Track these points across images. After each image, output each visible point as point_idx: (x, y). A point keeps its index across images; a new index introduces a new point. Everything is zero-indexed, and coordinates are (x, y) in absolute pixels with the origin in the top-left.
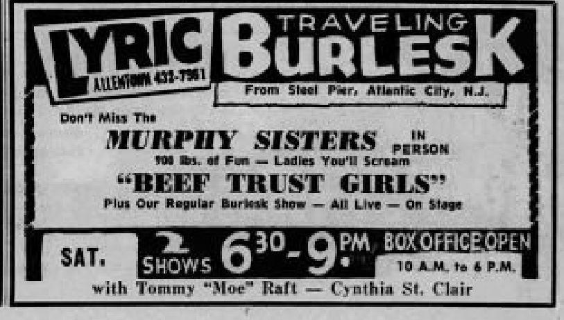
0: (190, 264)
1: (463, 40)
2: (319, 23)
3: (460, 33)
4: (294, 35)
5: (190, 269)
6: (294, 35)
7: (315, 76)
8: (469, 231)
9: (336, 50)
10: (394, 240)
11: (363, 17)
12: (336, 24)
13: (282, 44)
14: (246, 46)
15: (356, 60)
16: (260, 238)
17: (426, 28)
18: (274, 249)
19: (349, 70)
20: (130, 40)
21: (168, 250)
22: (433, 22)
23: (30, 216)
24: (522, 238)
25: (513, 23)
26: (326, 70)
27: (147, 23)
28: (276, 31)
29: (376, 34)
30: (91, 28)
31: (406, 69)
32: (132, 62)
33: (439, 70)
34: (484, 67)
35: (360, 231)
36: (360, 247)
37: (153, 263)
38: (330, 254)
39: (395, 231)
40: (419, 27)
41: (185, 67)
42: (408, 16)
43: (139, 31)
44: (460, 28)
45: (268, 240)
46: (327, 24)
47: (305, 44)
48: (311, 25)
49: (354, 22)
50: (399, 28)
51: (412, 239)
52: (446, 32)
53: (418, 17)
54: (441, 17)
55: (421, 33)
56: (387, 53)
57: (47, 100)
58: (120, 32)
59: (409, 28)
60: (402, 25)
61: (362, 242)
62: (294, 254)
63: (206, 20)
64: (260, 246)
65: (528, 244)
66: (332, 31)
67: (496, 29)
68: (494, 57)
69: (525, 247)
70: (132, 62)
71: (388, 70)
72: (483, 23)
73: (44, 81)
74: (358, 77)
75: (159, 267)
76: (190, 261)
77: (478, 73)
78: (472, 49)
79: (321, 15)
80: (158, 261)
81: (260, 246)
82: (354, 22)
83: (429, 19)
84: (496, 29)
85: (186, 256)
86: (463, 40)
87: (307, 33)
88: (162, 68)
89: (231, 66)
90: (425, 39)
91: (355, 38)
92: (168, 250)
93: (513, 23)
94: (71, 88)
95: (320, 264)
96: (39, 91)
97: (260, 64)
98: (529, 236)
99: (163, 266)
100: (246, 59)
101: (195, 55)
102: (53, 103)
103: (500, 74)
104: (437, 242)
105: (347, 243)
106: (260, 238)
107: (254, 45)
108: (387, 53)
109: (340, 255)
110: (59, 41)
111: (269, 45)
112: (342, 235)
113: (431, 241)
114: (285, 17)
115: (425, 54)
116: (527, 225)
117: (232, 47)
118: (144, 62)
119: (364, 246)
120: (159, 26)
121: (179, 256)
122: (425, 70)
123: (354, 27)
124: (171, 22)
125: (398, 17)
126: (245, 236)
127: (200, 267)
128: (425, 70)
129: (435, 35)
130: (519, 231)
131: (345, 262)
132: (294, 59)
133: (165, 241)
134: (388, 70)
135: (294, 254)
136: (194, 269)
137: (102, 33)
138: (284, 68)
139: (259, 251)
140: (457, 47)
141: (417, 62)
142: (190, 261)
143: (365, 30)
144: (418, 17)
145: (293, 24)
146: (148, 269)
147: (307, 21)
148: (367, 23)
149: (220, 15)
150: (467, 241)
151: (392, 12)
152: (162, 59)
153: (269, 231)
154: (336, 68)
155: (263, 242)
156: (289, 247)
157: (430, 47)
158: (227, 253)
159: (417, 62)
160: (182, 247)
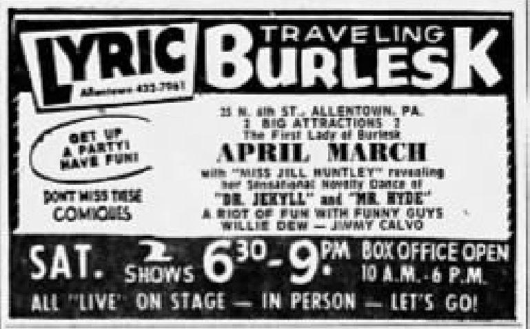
1: (443, 52)
2: (302, 36)
3: (438, 45)
4: (277, 45)
5: (172, 279)
6: (277, 45)
7: (296, 89)
8: (447, 241)
9: (319, 61)
10: (372, 248)
11: (343, 29)
12: (319, 35)
13: (265, 54)
14: (229, 57)
15: (338, 72)
16: (241, 246)
17: (404, 40)
18: (256, 258)
19: (330, 81)
20: (114, 49)
21: (150, 258)
22: (412, 36)
23: (14, 222)
24: (499, 248)
25: (492, 35)
26: (308, 81)
27: (132, 32)
28: (259, 41)
29: (357, 46)
30: (76, 36)
31: (384, 80)
32: (116, 71)
33: (417, 82)
34: (462, 80)
35: (340, 239)
36: (340, 255)
37: (136, 271)
38: (312, 262)
39: (373, 240)
40: (397, 38)
42: (387, 28)
43: (123, 40)
44: (439, 39)
45: (249, 248)
46: (310, 36)
47: (288, 55)
48: (294, 36)
49: (336, 32)
50: (378, 39)
51: (389, 246)
52: (423, 44)
53: (396, 29)
54: (419, 29)
55: (399, 44)
56: (366, 65)
57: (33, 108)
58: (105, 40)
59: (387, 40)
60: (382, 36)
61: (342, 250)
62: (276, 263)
63: (191, 30)
64: (241, 255)
65: (506, 255)
66: (315, 43)
67: (475, 40)
68: (472, 68)
69: (502, 259)
70: (116, 71)
71: (367, 81)
72: (462, 35)
73: (28, 87)
74: (339, 89)
75: (141, 275)
76: (172, 269)
77: (457, 84)
78: (450, 61)
79: (305, 26)
80: (140, 269)
81: (241, 255)
82: (336, 32)
83: (407, 30)
84: (475, 40)
86: (443, 52)
87: (290, 43)
89: (214, 76)
90: (403, 51)
91: (336, 49)
92: (150, 258)
93: (492, 35)
94: (56, 95)
95: (301, 272)
96: (24, 98)
97: (243, 74)
98: (507, 247)
100: (229, 70)
101: (175, 65)
102: (39, 111)
103: (478, 87)
104: (415, 251)
106: (241, 246)
107: (237, 57)
108: (366, 65)
109: (322, 263)
110: (44, 48)
111: (252, 56)
112: (324, 243)
114: (268, 29)
115: (402, 65)
116: (505, 235)
117: (215, 57)
118: (127, 71)
120: (143, 37)
122: (402, 81)
123: (336, 39)
124: (155, 31)
125: (377, 29)
126: (226, 244)
127: (182, 276)
128: (402, 81)
129: (414, 47)
130: (495, 242)
131: (327, 270)
132: (276, 71)
133: (147, 250)
134: (367, 81)
135: (276, 263)
136: (177, 278)
137: (87, 42)
138: (267, 80)
139: (241, 259)
140: (435, 59)
141: (395, 74)
142: (172, 269)
143: (346, 41)
144: (396, 29)
145: (276, 35)
146: (129, 277)
147: (290, 32)
148: (348, 35)
149: (204, 26)
150: (444, 251)
151: (371, 24)
152: (146, 68)
153: (250, 239)
154: (319, 80)
156: (268, 258)
157: (408, 59)
158: (209, 261)
159: (395, 74)
160: (165, 255)
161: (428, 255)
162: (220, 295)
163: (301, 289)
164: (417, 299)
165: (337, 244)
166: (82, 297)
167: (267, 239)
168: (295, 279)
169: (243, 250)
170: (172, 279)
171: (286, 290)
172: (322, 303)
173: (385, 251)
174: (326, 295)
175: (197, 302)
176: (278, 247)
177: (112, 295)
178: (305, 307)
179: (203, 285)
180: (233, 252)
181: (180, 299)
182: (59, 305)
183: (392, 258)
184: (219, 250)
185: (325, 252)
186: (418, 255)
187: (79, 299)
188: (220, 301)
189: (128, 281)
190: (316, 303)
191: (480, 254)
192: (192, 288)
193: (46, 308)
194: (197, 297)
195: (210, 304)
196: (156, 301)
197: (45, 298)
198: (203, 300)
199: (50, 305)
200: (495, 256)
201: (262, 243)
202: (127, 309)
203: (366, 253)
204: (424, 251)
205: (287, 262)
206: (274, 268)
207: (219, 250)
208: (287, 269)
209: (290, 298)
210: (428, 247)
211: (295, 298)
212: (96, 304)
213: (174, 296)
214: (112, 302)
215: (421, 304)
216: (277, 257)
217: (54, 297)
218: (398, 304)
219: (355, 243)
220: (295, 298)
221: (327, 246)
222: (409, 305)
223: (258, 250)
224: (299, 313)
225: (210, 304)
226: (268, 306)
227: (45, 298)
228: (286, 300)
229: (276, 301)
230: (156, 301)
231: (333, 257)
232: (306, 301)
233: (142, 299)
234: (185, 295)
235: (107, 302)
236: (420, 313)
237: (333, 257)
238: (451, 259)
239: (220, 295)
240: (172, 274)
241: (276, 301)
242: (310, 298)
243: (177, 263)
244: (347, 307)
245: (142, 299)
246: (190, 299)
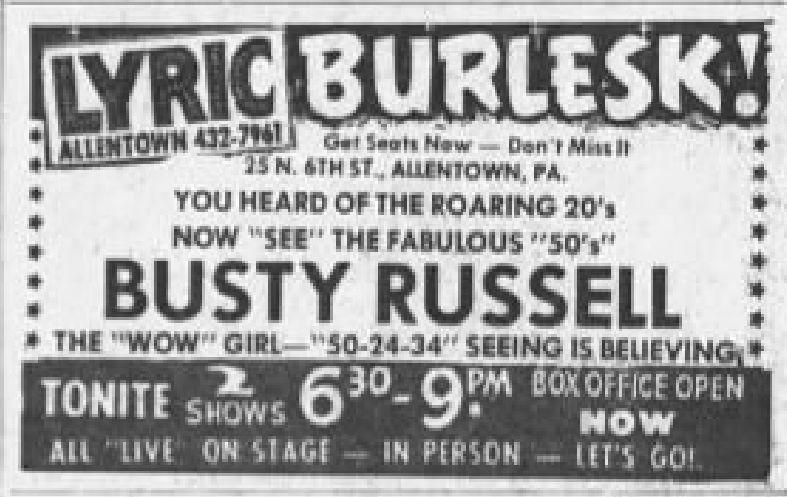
16: (355, 375)
18: (376, 391)
21: (224, 390)
35: (497, 369)
38: (454, 397)
45: (367, 378)
51: (572, 381)
62: (402, 399)
64: (356, 386)
69: (733, 395)
75: (210, 414)
76: (254, 405)
80: (209, 406)
81: (356, 386)
85: (249, 400)
88: (218, 124)
92: (224, 390)
105: (479, 383)
109: (467, 401)
112: (471, 374)
113: (601, 384)
119: (502, 386)
121: (240, 399)
126: (335, 372)
127: (269, 415)
131: (475, 409)
133: (222, 379)
135: (402, 399)
136: (261, 418)
139: (355, 394)
142: (254, 405)
150: (650, 385)
155: (360, 381)
156: (396, 387)
158: (308, 396)
160: (245, 385)
162: (324, 442)
163: (438, 435)
164: (612, 453)
165: (491, 376)
167: (391, 365)
168: (432, 423)
169: (360, 381)
171: (417, 435)
172: (468, 455)
174: (474, 444)
175: (290, 454)
176: (408, 376)
178: (443, 461)
181: (266, 447)
182: (90, 453)
183: (577, 393)
186: (614, 390)
188: (323, 451)
189: (192, 421)
192: (281, 433)
194: (290, 445)
196: (230, 449)
197: (71, 445)
198: (297, 449)
199: (77, 453)
200: (722, 392)
202: (189, 461)
203: (539, 386)
205: (417, 394)
206: (401, 406)
212: (144, 454)
214: (167, 451)
215: (617, 458)
216: (403, 391)
218: (586, 457)
222: (600, 460)
223: (379, 380)
224: (434, 469)
227: (71, 445)
229: (401, 451)
231: (486, 389)
233: (212, 450)
234: (273, 442)
235: (160, 454)
236: (616, 472)
237: (486, 389)
239: (324, 442)
240: (255, 413)
242: (449, 448)
245: (212, 450)
246: (281, 448)
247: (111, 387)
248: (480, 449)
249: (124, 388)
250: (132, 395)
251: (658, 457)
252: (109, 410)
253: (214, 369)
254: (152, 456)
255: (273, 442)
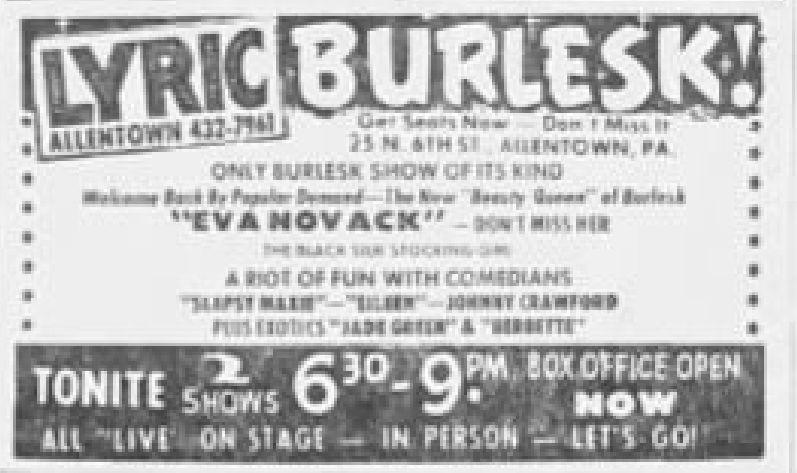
0: (250, 401)
5: (250, 406)
18: (371, 378)
36: (495, 373)
37: (198, 397)
38: (454, 383)
41: (244, 112)
45: (362, 364)
51: (567, 361)
61: (496, 367)
62: (401, 386)
64: (350, 374)
69: (731, 373)
81: (350, 374)
99: (214, 402)
104: (606, 367)
109: (466, 385)
112: (470, 357)
121: (235, 388)
126: (327, 359)
127: (264, 404)
133: (217, 366)
135: (401, 386)
136: (256, 407)
139: (349, 381)
150: (649, 366)
153: (364, 351)
155: (354, 368)
158: (301, 383)
160: (242, 373)
161: (626, 373)
163: (438, 421)
165: (489, 358)
166: (118, 434)
168: (430, 408)
169: (354, 368)
170: (250, 406)
171: (415, 420)
172: (469, 440)
173: (561, 368)
174: (473, 429)
176: (405, 363)
177: (163, 430)
178: (444, 445)
179: (291, 415)
180: (337, 372)
181: (261, 435)
184: (319, 369)
185: (471, 370)
187: (112, 438)
188: (319, 439)
189: (188, 411)
190: (459, 440)
191: (699, 369)
193: (64, 447)
194: (284, 435)
195: (303, 442)
199: (69, 442)
200: (722, 370)
201: (382, 358)
204: (620, 368)
206: (399, 394)
207: (319, 369)
208: (421, 394)
209: (422, 437)
210: (627, 362)
211: (430, 433)
213: (252, 433)
214: (162, 439)
216: (400, 378)
217: (75, 434)
219: (517, 356)
220: (430, 433)
221: (474, 362)
222: (598, 442)
223: (376, 367)
225: (303, 442)
226: (390, 444)
228: (417, 437)
229: (400, 438)
230: (228, 439)
231: (484, 376)
232: (444, 438)
234: (268, 430)
235: (155, 444)
238: (660, 377)
239: (318, 430)
240: (250, 401)
241: (400, 438)
243: (258, 386)
244: (505, 445)
245: (209, 438)
246: (275, 437)
247: (104, 375)
248: (480, 433)
249: (117, 377)
250: (125, 384)
251: (660, 436)
252: (102, 401)
253: (209, 356)
254: (147, 443)
255: (268, 430)
